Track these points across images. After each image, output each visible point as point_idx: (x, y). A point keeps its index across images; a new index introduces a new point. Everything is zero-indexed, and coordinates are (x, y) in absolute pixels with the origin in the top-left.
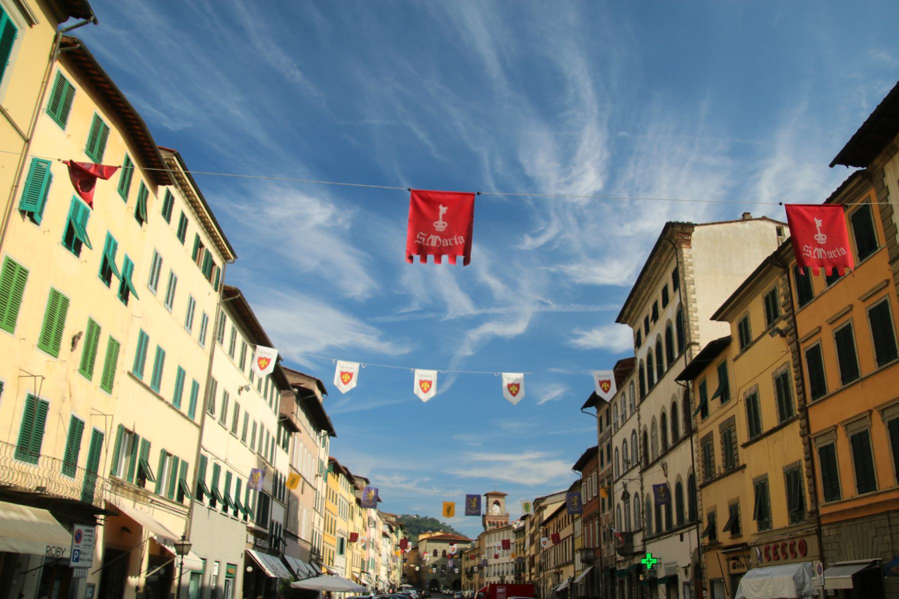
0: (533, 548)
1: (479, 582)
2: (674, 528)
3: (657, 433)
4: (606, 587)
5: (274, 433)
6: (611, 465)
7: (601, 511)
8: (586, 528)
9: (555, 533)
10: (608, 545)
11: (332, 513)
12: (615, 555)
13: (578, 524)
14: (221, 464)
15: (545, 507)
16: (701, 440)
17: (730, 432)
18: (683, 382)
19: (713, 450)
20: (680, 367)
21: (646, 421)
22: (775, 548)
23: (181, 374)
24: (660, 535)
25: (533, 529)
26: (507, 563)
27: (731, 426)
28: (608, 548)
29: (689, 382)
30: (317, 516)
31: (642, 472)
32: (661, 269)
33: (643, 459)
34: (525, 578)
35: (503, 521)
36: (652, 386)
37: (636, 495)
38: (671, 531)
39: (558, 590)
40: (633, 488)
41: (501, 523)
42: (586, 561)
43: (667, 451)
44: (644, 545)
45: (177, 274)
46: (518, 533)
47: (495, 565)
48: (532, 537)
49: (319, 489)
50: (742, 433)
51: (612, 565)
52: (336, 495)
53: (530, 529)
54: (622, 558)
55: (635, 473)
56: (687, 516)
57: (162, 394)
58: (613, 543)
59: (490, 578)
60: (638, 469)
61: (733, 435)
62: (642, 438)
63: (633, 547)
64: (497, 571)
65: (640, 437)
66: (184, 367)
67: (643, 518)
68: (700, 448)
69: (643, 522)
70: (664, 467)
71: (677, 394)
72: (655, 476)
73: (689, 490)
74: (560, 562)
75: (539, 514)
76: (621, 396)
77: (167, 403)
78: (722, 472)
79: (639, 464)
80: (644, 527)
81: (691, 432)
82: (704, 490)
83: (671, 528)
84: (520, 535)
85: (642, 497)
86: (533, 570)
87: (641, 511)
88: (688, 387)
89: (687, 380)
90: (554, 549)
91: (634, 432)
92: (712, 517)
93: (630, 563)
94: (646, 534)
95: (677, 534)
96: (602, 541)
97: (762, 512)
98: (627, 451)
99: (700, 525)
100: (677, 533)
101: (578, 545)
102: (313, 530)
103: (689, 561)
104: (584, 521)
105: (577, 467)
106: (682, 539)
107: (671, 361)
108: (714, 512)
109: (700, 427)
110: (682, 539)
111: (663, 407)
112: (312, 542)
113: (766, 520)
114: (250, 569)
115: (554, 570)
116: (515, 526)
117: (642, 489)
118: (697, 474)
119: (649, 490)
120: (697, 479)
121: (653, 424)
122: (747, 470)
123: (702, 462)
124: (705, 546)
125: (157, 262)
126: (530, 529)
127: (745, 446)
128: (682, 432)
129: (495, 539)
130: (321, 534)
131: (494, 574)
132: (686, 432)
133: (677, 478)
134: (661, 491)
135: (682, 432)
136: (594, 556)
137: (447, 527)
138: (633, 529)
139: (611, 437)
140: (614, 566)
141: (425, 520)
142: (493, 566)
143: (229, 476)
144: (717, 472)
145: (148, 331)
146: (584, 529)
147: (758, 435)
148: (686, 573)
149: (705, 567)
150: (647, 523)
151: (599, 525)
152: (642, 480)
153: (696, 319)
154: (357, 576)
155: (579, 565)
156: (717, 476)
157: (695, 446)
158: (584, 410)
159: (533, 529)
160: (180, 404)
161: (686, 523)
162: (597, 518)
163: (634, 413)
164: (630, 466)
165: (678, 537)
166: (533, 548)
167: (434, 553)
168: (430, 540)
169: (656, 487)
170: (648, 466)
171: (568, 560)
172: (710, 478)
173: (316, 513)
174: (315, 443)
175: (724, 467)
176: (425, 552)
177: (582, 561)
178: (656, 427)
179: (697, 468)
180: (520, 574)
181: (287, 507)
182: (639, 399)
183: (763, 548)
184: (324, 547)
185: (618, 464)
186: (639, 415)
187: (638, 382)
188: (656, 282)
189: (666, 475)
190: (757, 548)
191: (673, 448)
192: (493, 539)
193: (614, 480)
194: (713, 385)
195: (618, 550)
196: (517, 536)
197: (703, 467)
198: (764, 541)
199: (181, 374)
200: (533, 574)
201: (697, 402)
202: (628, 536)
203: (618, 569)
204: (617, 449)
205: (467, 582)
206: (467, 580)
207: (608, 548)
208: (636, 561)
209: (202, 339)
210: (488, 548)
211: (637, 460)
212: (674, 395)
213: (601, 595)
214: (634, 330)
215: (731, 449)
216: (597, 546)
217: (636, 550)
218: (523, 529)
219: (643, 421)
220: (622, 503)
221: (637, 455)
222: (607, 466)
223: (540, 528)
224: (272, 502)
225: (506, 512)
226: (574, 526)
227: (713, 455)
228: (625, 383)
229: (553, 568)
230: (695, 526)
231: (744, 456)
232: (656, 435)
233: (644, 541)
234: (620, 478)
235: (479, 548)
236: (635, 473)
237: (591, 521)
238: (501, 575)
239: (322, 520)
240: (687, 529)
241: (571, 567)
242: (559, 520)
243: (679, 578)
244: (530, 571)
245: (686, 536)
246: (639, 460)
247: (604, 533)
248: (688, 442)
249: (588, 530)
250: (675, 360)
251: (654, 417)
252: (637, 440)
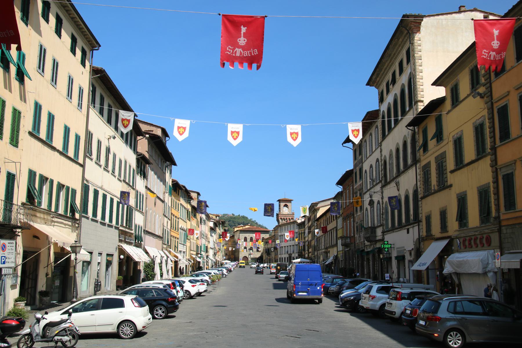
0: (310, 235)
1: (275, 258)
2: (403, 225)
3: (393, 161)
4: (358, 261)
5: (134, 165)
6: (362, 182)
7: (355, 212)
8: (345, 223)
9: (325, 226)
10: (360, 234)
11: (176, 217)
12: (364, 241)
13: (340, 220)
14: (98, 189)
15: (318, 209)
16: (422, 167)
17: (442, 163)
18: (411, 128)
19: (430, 174)
20: (410, 117)
21: (386, 153)
22: (470, 240)
23: (67, 130)
24: (393, 229)
25: (310, 223)
26: (293, 246)
27: (443, 158)
28: (360, 236)
29: (416, 127)
30: (166, 219)
31: (383, 187)
32: (398, 48)
33: (383, 178)
34: (305, 255)
35: (290, 218)
36: (390, 129)
37: (379, 202)
38: (401, 226)
39: (327, 263)
40: (376, 198)
41: (289, 219)
42: (345, 245)
43: (399, 173)
44: (383, 235)
45: (58, 59)
46: (300, 226)
47: (285, 247)
48: (310, 228)
49: (166, 201)
50: (450, 164)
51: (362, 248)
52: (178, 204)
53: (308, 223)
54: (369, 243)
55: (378, 188)
56: (412, 218)
57: (54, 144)
58: (363, 234)
60: (380, 185)
61: (444, 164)
62: (383, 165)
63: (376, 236)
65: (381, 164)
66: (69, 125)
67: (383, 218)
68: (422, 173)
69: (383, 221)
70: (397, 184)
71: (407, 136)
72: (391, 191)
73: (413, 200)
74: (328, 245)
75: (314, 213)
76: (369, 135)
77: (58, 151)
78: (436, 189)
79: (381, 181)
80: (383, 223)
81: (415, 161)
82: (424, 200)
83: (401, 225)
84: (302, 227)
85: (383, 204)
86: (310, 250)
87: (382, 213)
88: (414, 131)
89: (414, 126)
90: (324, 237)
91: (377, 160)
92: (428, 219)
93: (374, 246)
94: (384, 228)
95: (405, 229)
96: (356, 232)
97: (462, 216)
98: (373, 173)
99: (421, 223)
100: (405, 228)
101: (340, 234)
102: (164, 228)
103: (413, 247)
104: (344, 218)
105: (339, 183)
106: (408, 232)
107: (404, 113)
108: (430, 215)
109: (422, 158)
110: (408, 232)
111: (398, 144)
112: (163, 236)
113: (465, 221)
114: (122, 257)
115: (324, 250)
116: (299, 221)
117: (382, 198)
118: (419, 190)
119: (386, 199)
120: (419, 193)
121: (391, 155)
122: (453, 188)
123: (423, 182)
124: (423, 237)
125: (42, 52)
126: (308, 223)
127: (452, 172)
128: (409, 161)
129: (285, 230)
130: (169, 230)
132: (412, 162)
133: (406, 192)
134: (394, 201)
135: (409, 161)
136: (350, 242)
137: (253, 221)
138: (376, 225)
139: (362, 163)
140: (363, 249)
141: (239, 217)
142: (284, 247)
143: (105, 197)
144: (433, 189)
145: (41, 102)
146: (344, 224)
147: (461, 165)
148: (411, 254)
149: (423, 251)
150: (385, 221)
151: (354, 221)
152: (382, 193)
153: (422, 85)
154: (194, 256)
155: (340, 247)
156: (433, 191)
157: (418, 171)
158: (344, 145)
159: (310, 223)
160: (67, 151)
161: (411, 222)
162: (352, 217)
163: (378, 148)
164: (375, 183)
165: (406, 231)
166: (310, 235)
167: (245, 239)
168: (242, 231)
169: (390, 198)
170: (386, 184)
171: (333, 244)
172: (428, 193)
173: (165, 218)
174: (163, 170)
175: (437, 186)
176: (239, 239)
177: (342, 245)
178: (392, 157)
179: (419, 185)
180: (302, 253)
181: (145, 214)
182: (381, 138)
183: (462, 240)
184: (171, 239)
185: (367, 181)
186: (381, 149)
187: (381, 126)
188: (394, 57)
189: (398, 190)
190: (458, 240)
191: (403, 172)
192: (284, 230)
193: (364, 192)
194: (432, 130)
195: (366, 238)
196: (299, 228)
197: (423, 185)
198: (463, 235)
199: (67, 130)
200: (311, 252)
201: (420, 141)
202: (373, 229)
203: (366, 250)
204: (366, 171)
205: (267, 258)
206: (267, 257)
207: (360, 236)
208: (378, 245)
209: (80, 105)
210: (280, 236)
211: (380, 179)
212: (405, 136)
213: (355, 266)
214: (379, 91)
215: (443, 174)
216: (352, 235)
217: (378, 238)
218: (303, 224)
219: (384, 153)
220: (369, 207)
221: (380, 176)
222: (359, 183)
223: (314, 223)
224: (135, 212)
225: (292, 212)
226: (337, 222)
227: (431, 177)
228: (372, 127)
229: (324, 249)
230: (417, 224)
231: (451, 179)
232: (392, 163)
233: (383, 232)
234: (368, 190)
235: (274, 235)
236: (378, 188)
237: (348, 219)
238: (289, 253)
239: (169, 222)
240: (412, 226)
241: (335, 249)
243: (406, 257)
244: (308, 250)
245: (411, 230)
246: (381, 179)
247: (357, 227)
248: (414, 168)
249: (346, 224)
250: (406, 112)
251: (391, 151)
252: (379, 166)
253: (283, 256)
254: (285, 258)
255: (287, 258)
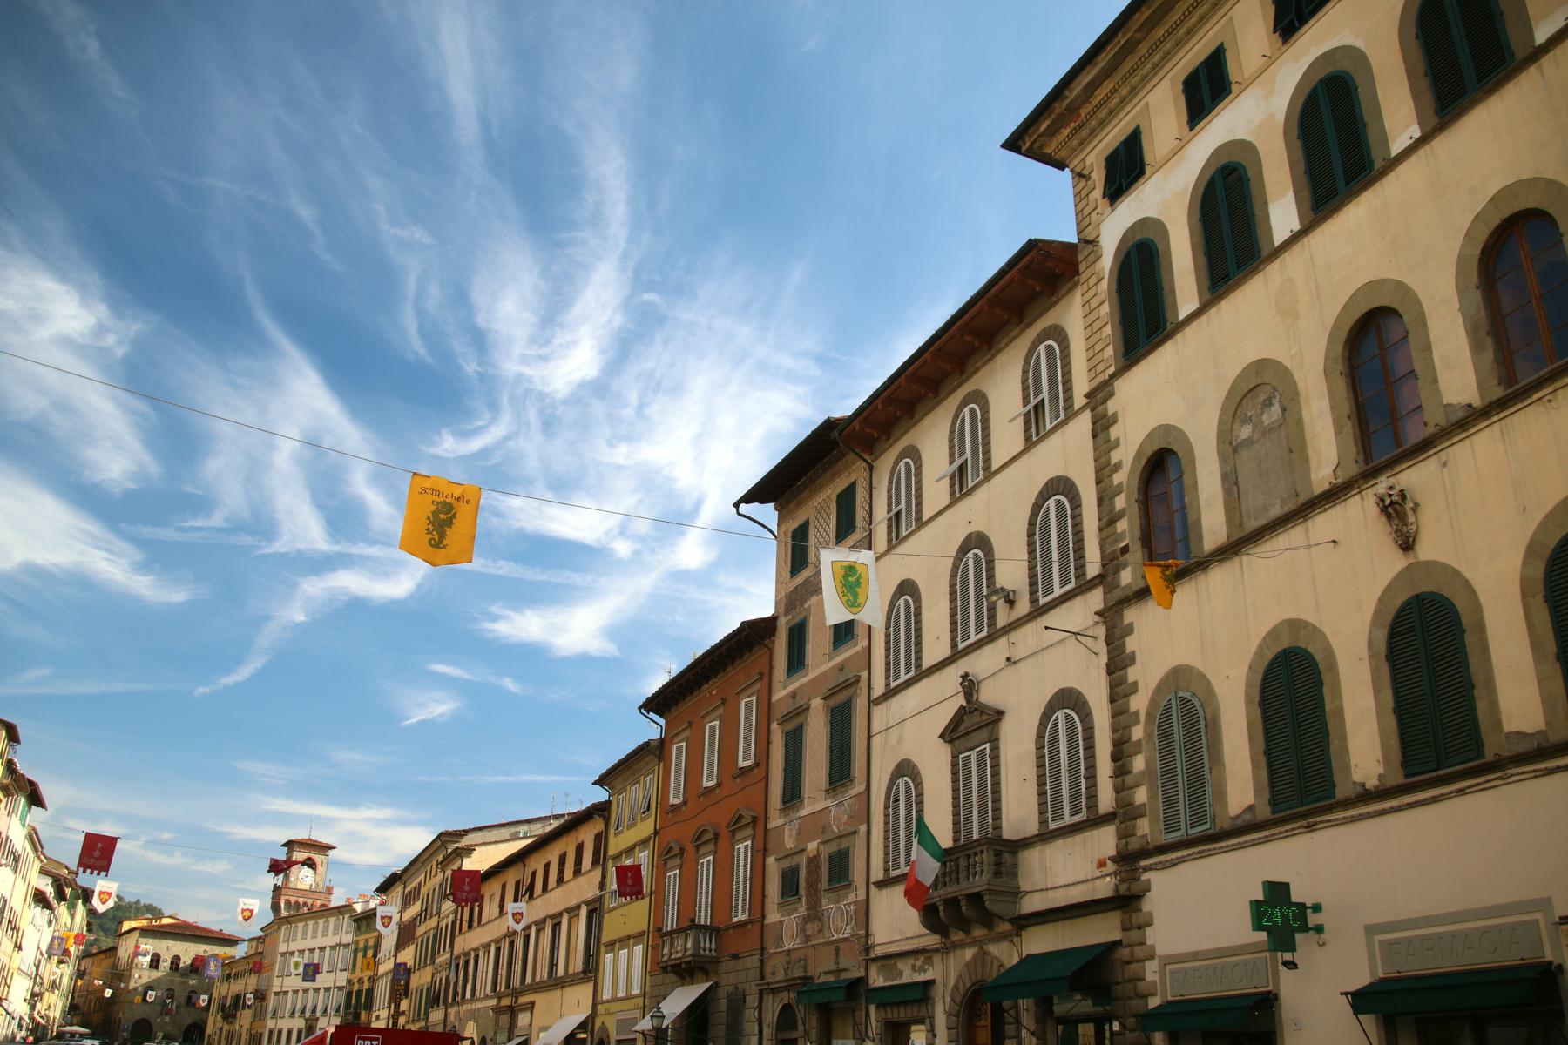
1: (249, 1031)
59: (280, 1021)
64: (299, 1007)
131: (293, 1014)
142: (290, 994)
205: (221, 1029)
242: (529, 871)
253: (285, 1024)
254: (290, 1032)
255: (300, 1032)
